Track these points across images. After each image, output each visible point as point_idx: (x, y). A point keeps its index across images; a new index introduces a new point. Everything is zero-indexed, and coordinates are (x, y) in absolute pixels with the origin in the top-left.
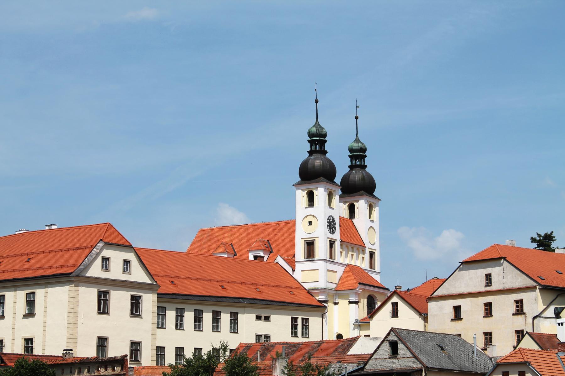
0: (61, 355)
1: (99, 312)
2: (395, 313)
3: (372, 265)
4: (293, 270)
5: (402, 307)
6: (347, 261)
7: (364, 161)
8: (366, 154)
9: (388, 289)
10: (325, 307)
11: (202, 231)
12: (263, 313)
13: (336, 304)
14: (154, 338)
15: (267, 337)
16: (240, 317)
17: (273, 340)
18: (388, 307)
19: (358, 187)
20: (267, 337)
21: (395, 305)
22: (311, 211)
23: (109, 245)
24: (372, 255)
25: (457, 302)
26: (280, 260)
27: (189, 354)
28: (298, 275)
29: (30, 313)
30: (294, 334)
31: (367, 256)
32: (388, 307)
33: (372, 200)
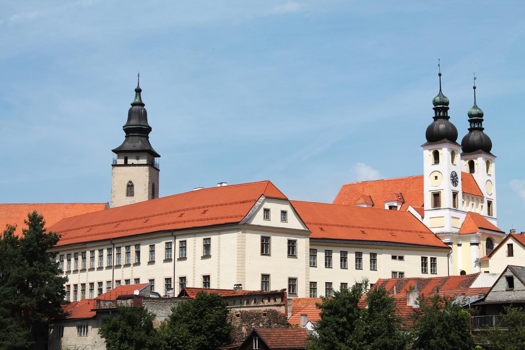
0: (233, 289)
1: (262, 254)
2: (510, 253)
3: (489, 212)
4: (423, 218)
5: (516, 247)
6: (468, 209)
7: (481, 124)
8: (483, 118)
9: (504, 233)
10: (450, 248)
11: (345, 186)
12: (398, 254)
13: (459, 245)
14: (307, 275)
15: (402, 274)
16: (378, 257)
17: (407, 276)
18: (505, 247)
19: (477, 146)
20: (402, 274)
21: (510, 246)
22: (436, 167)
23: (269, 198)
24: (489, 203)
26: (411, 209)
27: (337, 288)
28: (426, 222)
29: (207, 255)
30: (424, 271)
31: (485, 205)
32: (504, 248)
33: (489, 157)
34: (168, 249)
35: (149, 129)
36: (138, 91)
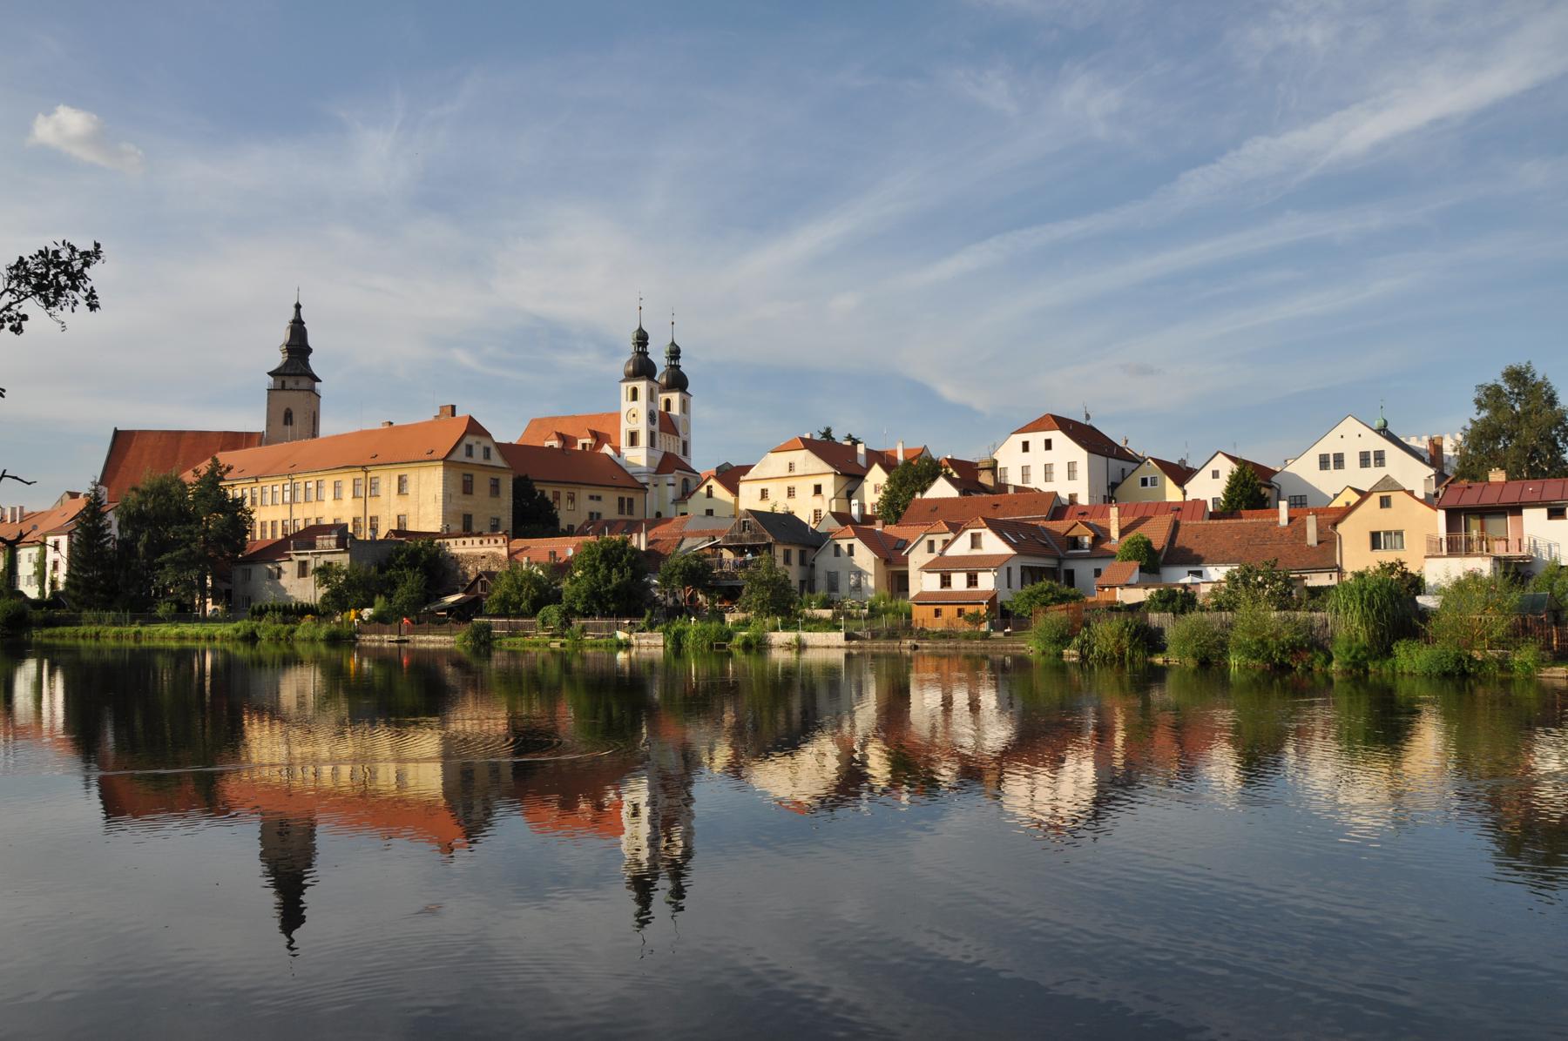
12: (596, 492)
15: (599, 515)
20: (599, 515)
21: (709, 488)
25: (764, 485)
29: (400, 491)
30: (621, 512)
34: (337, 486)
36: (298, 307)
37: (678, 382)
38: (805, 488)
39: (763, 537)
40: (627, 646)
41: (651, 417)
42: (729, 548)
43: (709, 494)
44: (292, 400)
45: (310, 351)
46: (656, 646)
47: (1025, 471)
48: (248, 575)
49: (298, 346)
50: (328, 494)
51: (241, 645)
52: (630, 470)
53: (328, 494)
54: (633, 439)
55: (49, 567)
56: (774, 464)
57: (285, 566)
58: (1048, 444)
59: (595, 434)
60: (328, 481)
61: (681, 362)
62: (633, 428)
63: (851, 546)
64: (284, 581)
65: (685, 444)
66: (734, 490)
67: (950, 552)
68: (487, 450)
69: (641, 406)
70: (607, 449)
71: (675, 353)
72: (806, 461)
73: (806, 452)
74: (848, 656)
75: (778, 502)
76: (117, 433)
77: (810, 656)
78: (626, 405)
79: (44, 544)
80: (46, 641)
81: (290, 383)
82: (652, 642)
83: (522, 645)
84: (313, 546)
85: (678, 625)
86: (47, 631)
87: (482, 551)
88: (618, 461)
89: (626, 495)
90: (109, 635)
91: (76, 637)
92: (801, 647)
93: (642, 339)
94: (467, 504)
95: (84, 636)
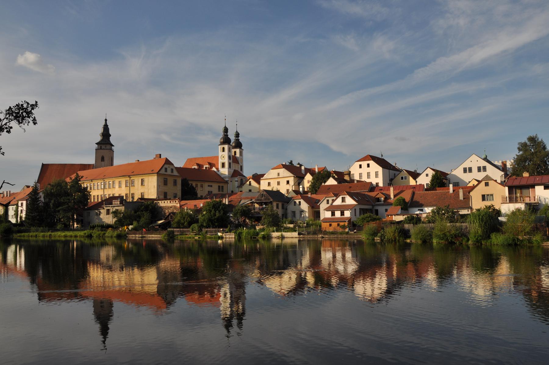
11: (188, 159)
12: (210, 184)
15: (211, 192)
20: (211, 192)
21: (250, 182)
25: (269, 181)
29: (142, 184)
30: (219, 191)
34: (120, 183)
35: (110, 135)
36: (106, 120)
37: (239, 145)
38: (283, 182)
39: (269, 199)
40: (221, 238)
41: (229, 157)
42: (257, 203)
43: (250, 184)
44: (105, 153)
45: (110, 135)
46: (232, 238)
47: (361, 175)
48: (89, 214)
49: (106, 134)
50: (117, 186)
51: (86, 239)
52: (222, 176)
53: (117, 186)
54: (223, 165)
55: (19, 212)
56: (273, 173)
57: (102, 211)
58: (368, 165)
59: (210, 164)
60: (117, 181)
61: (240, 138)
62: (223, 161)
63: (300, 202)
64: (101, 216)
65: (241, 167)
66: (259, 183)
67: (335, 204)
68: (172, 170)
69: (226, 154)
70: (214, 169)
71: (237, 135)
72: (284, 172)
73: (283, 169)
74: (299, 241)
75: (274, 187)
76: (43, 165)
77: (286, 241)
78: (221, 153)
79: (17, 205)
80: (18, 238)
81: (103, 147)
82: (231, 236)
83: (185, 238)
84: (112, 204)
85: (239, 230)
86: (19, 235)
87: (171, 205)
88: (218, 173)
89: (221, 185)
90: (40, 236)
91: (29, 236)
92: (283, 238)
93: (226, 130)
94: (165, 189)
95: (32, 236)
